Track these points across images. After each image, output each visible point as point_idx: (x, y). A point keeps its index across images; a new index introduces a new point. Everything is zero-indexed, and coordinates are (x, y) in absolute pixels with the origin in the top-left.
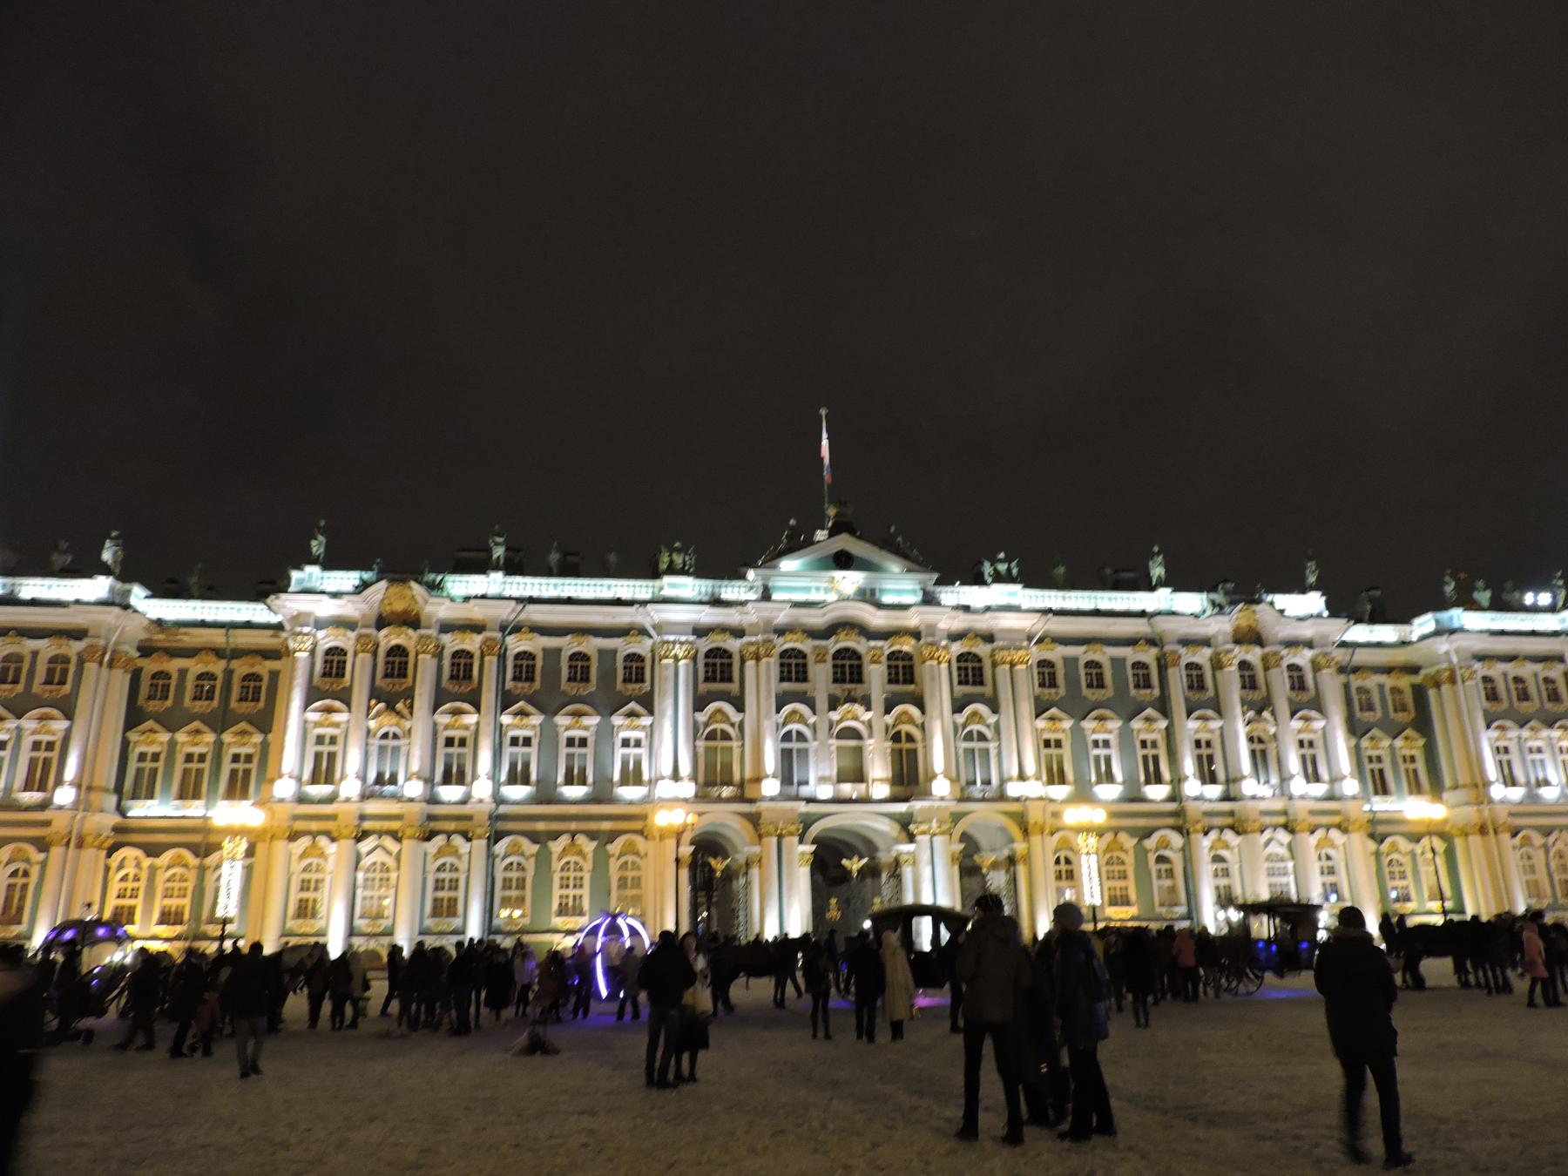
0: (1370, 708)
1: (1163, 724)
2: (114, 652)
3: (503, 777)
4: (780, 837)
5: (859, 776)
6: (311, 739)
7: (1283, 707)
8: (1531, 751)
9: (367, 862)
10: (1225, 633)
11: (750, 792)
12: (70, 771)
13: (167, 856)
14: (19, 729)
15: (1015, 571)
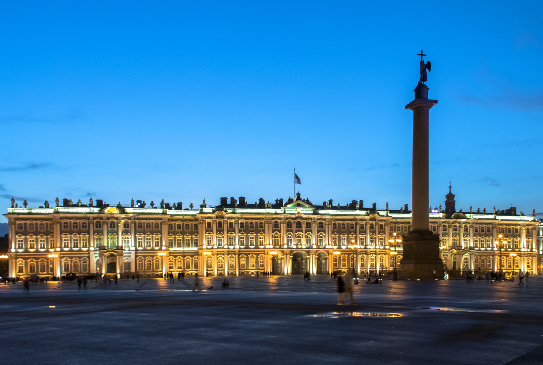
5: (301, 245)
7: (377, 232)
11: (282, 247)
13: (178, 257)
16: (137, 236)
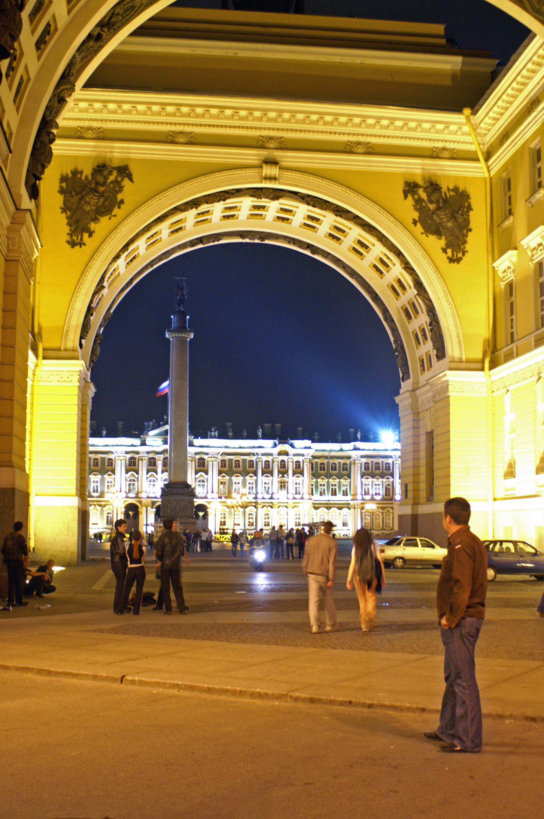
1: (255, 478)
4: (147, 507)
7: (290, 472)
8: (376, 485)
11: (140, 495)
15: (217, 435)
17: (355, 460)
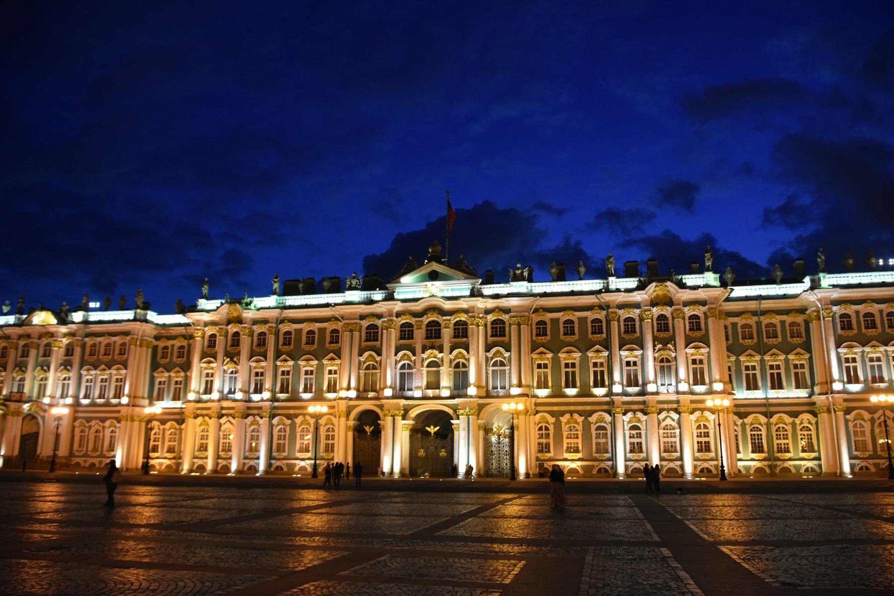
0: (775, 336)
1: (606, 354)
2: (142, 340)
3: (278, 389)
5: (437, 386)
6: (204, 374)
7: (680, 341)
8: (871, 360)
9: (223, 428)
10: (645, 300)
12: (126, 391)
14: (111, 374)
16: (84, 373)
17: (818, 311)
